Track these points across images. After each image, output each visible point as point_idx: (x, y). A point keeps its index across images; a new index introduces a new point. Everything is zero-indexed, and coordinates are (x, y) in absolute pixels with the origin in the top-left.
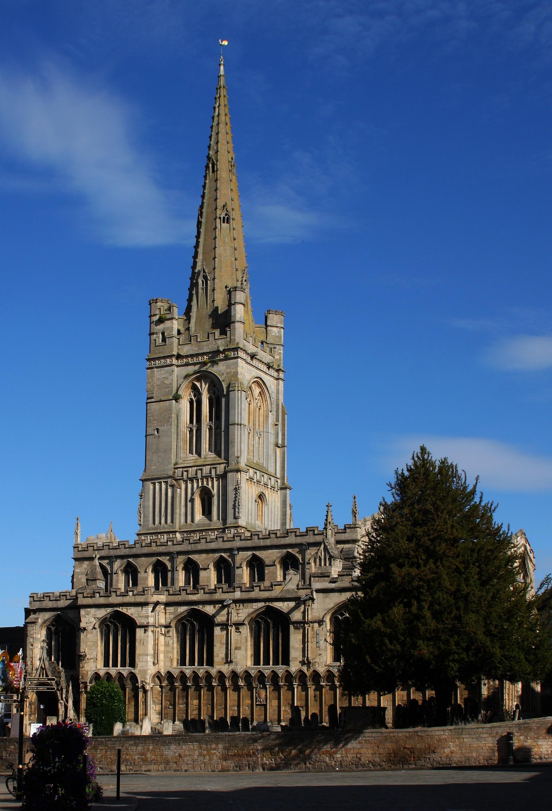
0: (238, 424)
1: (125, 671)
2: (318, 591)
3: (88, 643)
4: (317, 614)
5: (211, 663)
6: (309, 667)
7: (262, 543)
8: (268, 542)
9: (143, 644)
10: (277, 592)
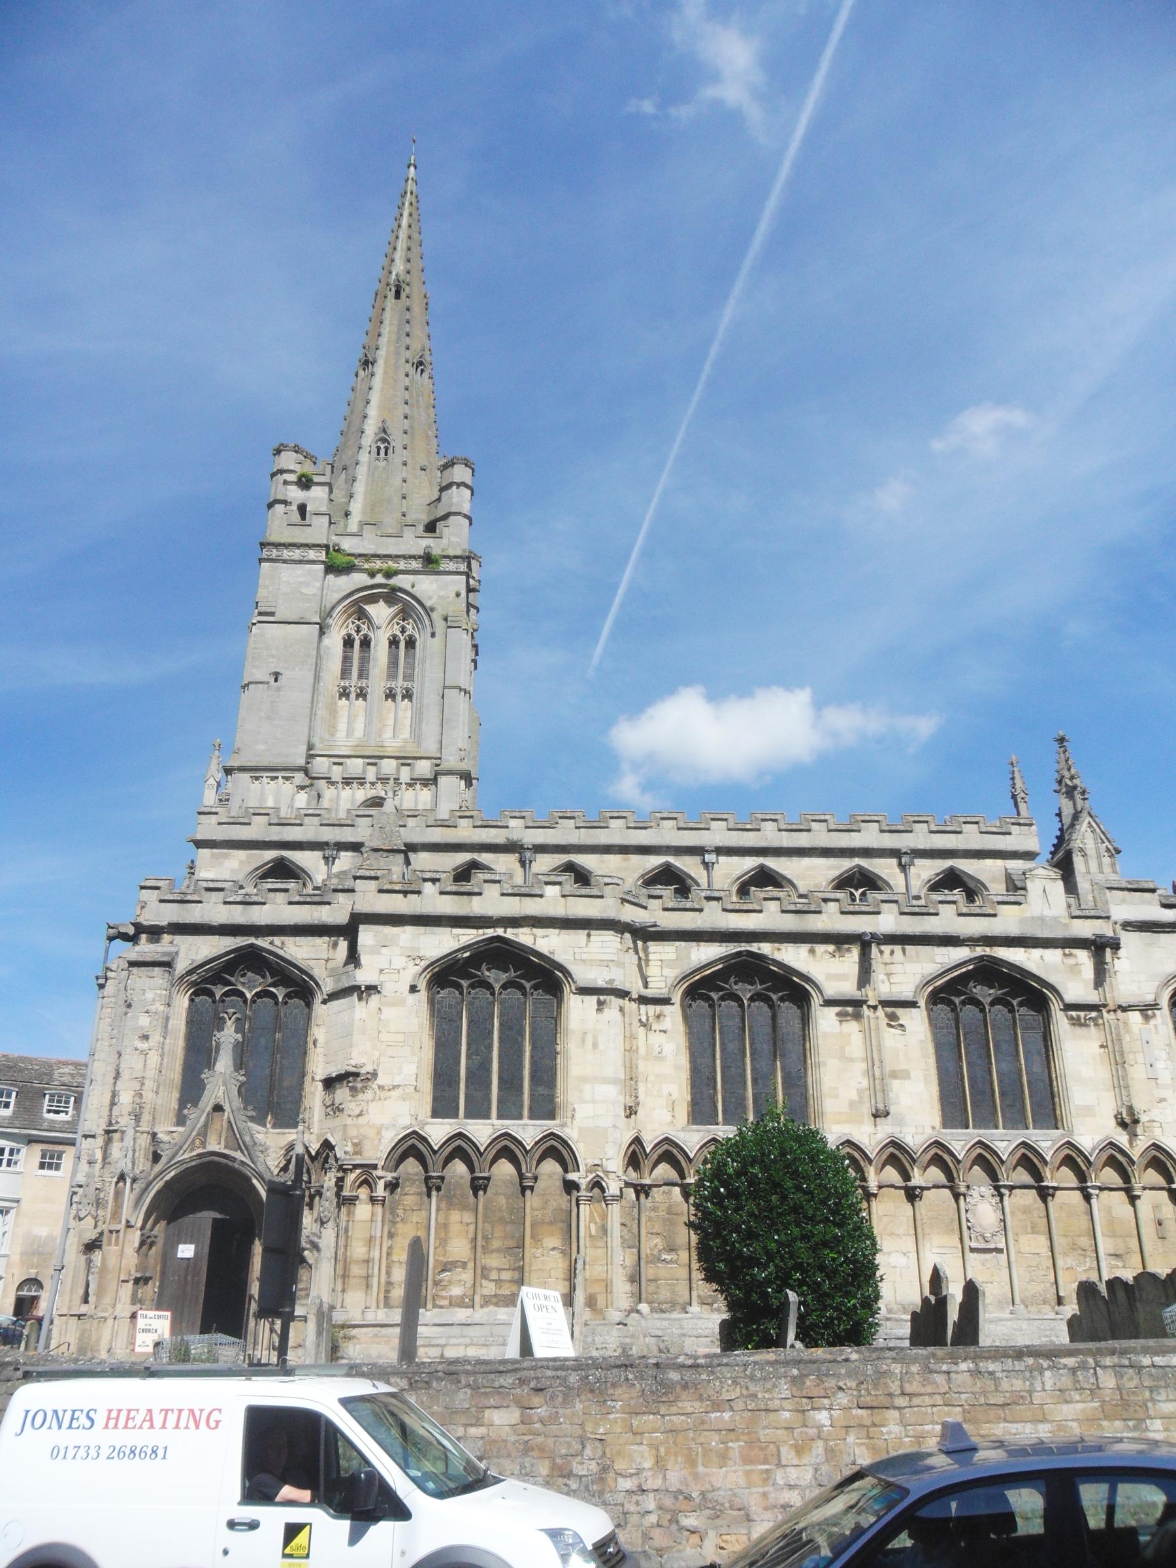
1: (528, 1131)
2: (1128, 925)
3: (383, 1037)
6: (1133, 1136)
8: (802, 840)
9: (595, 1046)
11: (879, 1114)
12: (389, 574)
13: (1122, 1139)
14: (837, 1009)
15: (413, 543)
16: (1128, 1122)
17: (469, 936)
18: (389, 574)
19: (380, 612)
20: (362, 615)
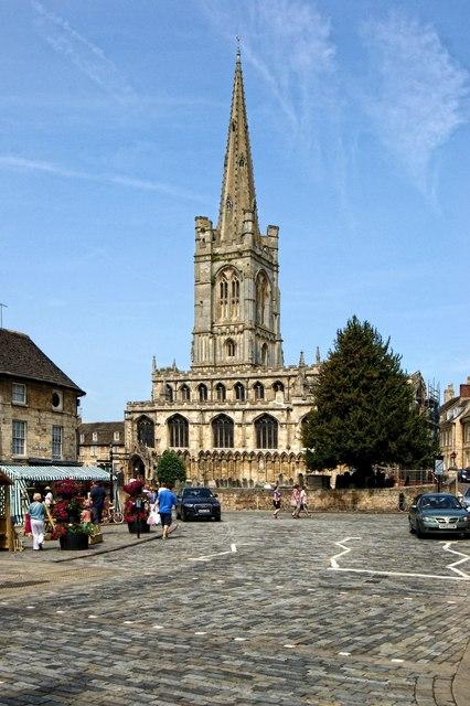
5: (232, 446)
7: (263, 374)
8: (266, 374)
10: (270, 405)
12: (230, 260)
13: (286, 451)
15: (235, 247)
16: (289, 448)
17: (173, 413)
18: (230, 260)
19: (228, 274)
20: (224, 276)
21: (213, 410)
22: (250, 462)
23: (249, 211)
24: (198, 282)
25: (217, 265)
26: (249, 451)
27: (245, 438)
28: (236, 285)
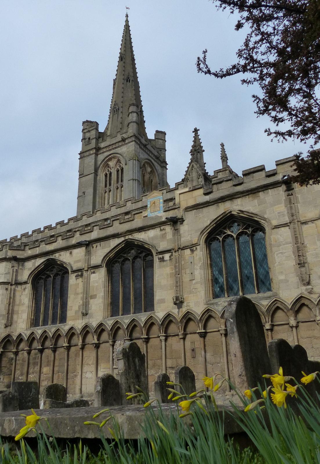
0: (135, 180)
2: (188, 209)
4: (189, 238)
5: (63, 320)
11: (85, 314)
13: (175, 311)
14: (75, 274)
16: (179, 302)
19: (112, 164)
21: (35, 257)
22: (97, 346)
23: (133, 105)
24: (82, 175)
25: (101, 157)
26: (94, 323)
27: (87, 297)
28: (121, 172)
